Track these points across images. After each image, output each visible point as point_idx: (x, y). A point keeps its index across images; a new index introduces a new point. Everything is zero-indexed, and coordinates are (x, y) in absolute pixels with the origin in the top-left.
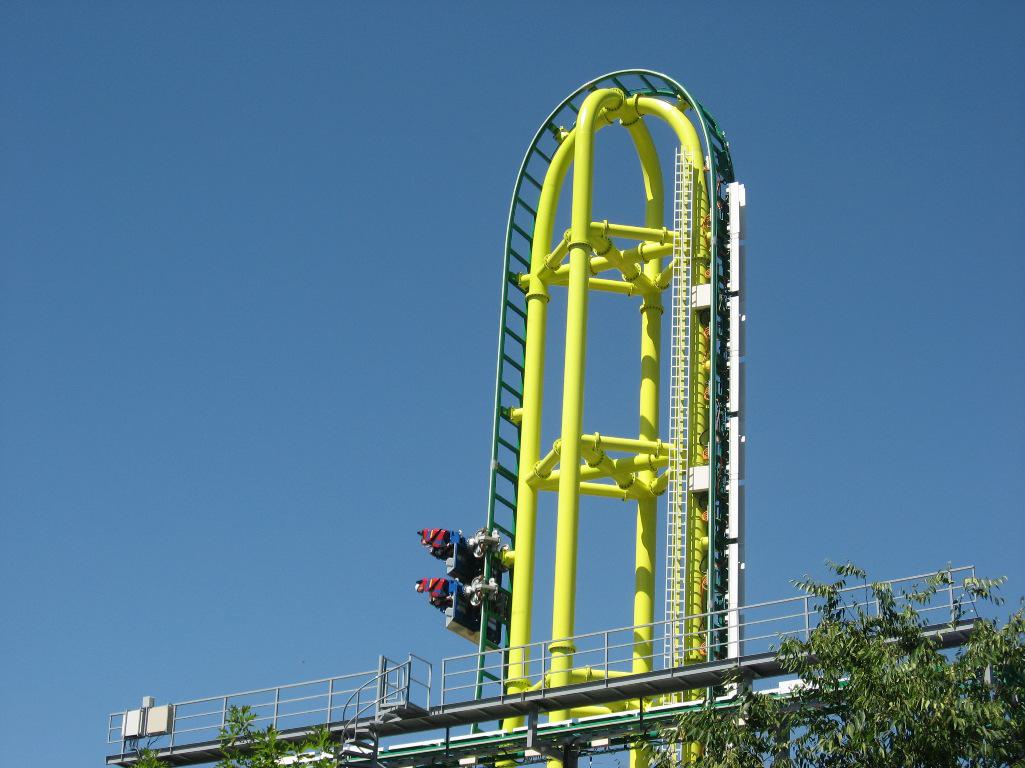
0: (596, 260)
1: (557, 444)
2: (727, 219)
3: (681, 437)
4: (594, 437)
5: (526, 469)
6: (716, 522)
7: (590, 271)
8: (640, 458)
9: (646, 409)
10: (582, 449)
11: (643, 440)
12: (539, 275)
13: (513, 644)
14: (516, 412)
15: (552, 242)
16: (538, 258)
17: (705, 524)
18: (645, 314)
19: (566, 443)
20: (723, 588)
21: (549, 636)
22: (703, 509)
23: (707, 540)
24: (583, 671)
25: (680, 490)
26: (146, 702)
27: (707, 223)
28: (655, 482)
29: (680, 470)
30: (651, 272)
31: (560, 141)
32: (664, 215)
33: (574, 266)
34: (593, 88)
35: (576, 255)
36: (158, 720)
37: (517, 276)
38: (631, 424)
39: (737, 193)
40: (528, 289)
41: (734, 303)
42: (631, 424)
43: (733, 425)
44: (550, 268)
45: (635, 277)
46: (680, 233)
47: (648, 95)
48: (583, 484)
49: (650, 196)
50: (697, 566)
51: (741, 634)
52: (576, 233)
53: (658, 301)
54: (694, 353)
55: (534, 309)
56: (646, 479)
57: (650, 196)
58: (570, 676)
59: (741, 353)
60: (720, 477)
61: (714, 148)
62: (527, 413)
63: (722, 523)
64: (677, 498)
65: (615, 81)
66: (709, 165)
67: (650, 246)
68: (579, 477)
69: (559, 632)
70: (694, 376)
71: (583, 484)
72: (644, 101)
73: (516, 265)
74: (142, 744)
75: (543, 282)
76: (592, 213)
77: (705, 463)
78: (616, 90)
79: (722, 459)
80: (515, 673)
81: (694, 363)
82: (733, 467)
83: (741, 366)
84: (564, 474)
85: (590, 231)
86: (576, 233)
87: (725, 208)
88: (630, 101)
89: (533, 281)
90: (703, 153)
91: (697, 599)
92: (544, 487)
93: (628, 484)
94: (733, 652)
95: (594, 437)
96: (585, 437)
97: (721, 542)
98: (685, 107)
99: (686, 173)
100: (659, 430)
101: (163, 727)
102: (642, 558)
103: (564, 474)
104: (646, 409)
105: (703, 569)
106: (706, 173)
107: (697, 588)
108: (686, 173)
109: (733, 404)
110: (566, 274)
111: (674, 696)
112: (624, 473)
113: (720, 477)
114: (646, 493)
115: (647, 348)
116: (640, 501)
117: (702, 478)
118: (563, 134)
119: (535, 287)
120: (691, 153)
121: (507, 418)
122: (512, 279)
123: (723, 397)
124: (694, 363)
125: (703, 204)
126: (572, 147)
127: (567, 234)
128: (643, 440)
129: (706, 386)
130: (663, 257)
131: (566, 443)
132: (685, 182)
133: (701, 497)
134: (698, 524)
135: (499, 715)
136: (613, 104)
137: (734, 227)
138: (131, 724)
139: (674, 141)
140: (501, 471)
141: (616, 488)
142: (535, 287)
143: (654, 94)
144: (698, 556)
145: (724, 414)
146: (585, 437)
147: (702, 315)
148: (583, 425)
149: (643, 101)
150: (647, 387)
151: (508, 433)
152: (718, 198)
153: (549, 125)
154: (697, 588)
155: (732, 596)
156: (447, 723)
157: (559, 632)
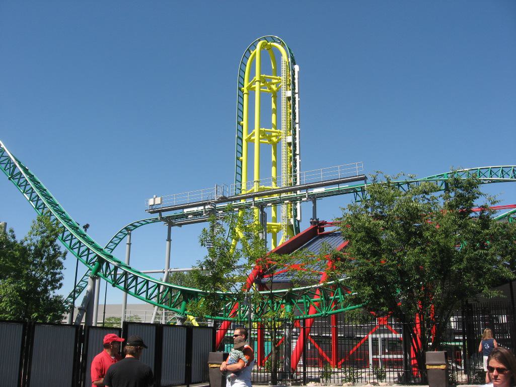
0: (262, 84)
1: (254, 131)
2: (294, 74)
3: (284, 129)
4: (263, 129)
5: (245, 137)
6: (293, 135)
7: (261, 87)
8: (274, 134)
9: (274, 121)
10: (260, 132)
11: (273, 129)
12: (247, 88)
13: (243, 182)
14: (242, 123)
15: (249, 81)
16: (246, 84)
17: (291, 151)
18: (273, 98)
19: (256, 130)
20: (295, 166)
21: (253, 179)
22: (290, 147)
23: (291, 154)
24: (263, 187)
25: (284, 142)
26: (155, 196)
27: (289, 75)
28: (277, 140)
29: (284, 137)
30: (274, 87)
31: (251, 54)
32: (278, 72)
33: (257, 85)
34: (259, 40)
35: (257, 83)
36: (158, 201)
37: (241, 88)
38: (270, 125)
39: (297, 68)
40: (243, 92)
41: (297, 96)
42: (270, 125)
43: (297, 126)
44: (249, 88)
45: (270, 89)
46: (283, 78)
47: (273, 42)
48: (261, 141)
49: (273, 68)
50: (289, 161)
51: (300, 179)
52: (257, 78)
53: (277, 95)
54: (287, 108)
55: (245, 97)
56: (274, 139)
57: (273, 68)
58: (259, 189)
59: (299, 108)
60: (294, 139)
61: (291, 56)
62: (244, 123)
63: (295, 150)
64: (284, 144)
65: (265, 39)
66: (290, 60)
67: (274, 81)
68: (260, 139)
69: (256, 178)
70: (287, 114)
71: (261, 141)
72: (272, 44)
73: (241, 86)
74: (154, 207)
75: (248, 90)
76: (261, 73)
77: (290, 90)
78: (265, 41)
79: (294, 134)
80: (244, 186)
81: (287, 110)
82: (297, 136)
83: (299, 111)
84: (256, 138)
85: (261, 77)
86: (257, 78)
87: (294, 71)
88: (269, 44)
89: (245, 90)
90: (288, 58)
91: (289, 169)
92: (250, 142)
93: (270, 141)
94: (298, 183)
95: (263, 129)
96: (261, 129)
97: (295, 155)
98: (283, 45)
99: (284, 62)
100: (278, 126)
101: (160, 203)
102: (273, 158)
103: (256, 138)
104: (274, 121)
105: (291, 161)
106: (289, 63)
107: (289, 166)
108: (284, 62)
109: (297, 121)
110: (255, 88)
111: (284, 194)
112: (269, 138)
113: (294, 139)
114: (274, 142)
115: (273, 106)
116: (273, 144)
117: (290, 139)
118: (251, 52)
119: (246, 91)
120: (285, 58)
121: (240, 124)
122: (240, 89)
123: (294, 119)
124: (287, 110)
125: (288, 70)
126: (255, 54)
127: (254, 78)
128: (273, 129)
129: (290, 116)
130: (277, 84)
131: (256, 130)
132: (284, 65)
133: (289, 144)
134: (289, 150)
135: (240, 199)
136: (265, 44)
137: (296, 76)
138: (151, 202)
139: (281, 55)
140: (238, 137)
141: (267, 141)
142: (246, 91)
143: (274, 42)
144: (289, 158)
145: (295, 123)
146: (261, 129)
147: (289, 99)
148: (260, 127)
149: (272, 44)
150: (274, 116)
151: (240, 128)
152: (292, 69)
153: (248, 50)
154: (289, 166)
155: (298, 168)
156: (232, 200)
157: (256, 178)
